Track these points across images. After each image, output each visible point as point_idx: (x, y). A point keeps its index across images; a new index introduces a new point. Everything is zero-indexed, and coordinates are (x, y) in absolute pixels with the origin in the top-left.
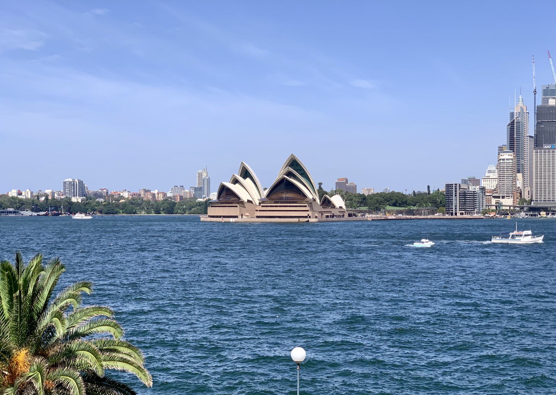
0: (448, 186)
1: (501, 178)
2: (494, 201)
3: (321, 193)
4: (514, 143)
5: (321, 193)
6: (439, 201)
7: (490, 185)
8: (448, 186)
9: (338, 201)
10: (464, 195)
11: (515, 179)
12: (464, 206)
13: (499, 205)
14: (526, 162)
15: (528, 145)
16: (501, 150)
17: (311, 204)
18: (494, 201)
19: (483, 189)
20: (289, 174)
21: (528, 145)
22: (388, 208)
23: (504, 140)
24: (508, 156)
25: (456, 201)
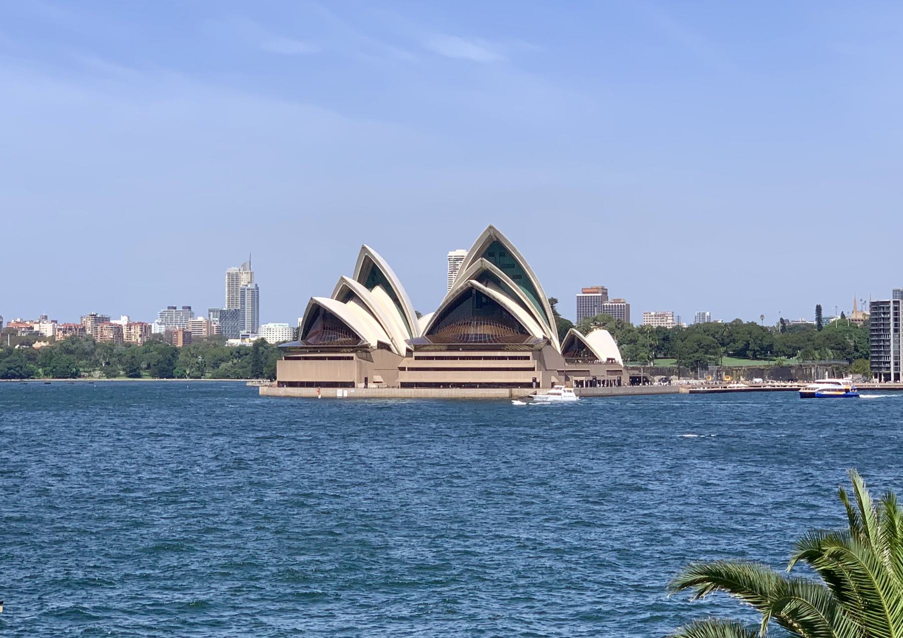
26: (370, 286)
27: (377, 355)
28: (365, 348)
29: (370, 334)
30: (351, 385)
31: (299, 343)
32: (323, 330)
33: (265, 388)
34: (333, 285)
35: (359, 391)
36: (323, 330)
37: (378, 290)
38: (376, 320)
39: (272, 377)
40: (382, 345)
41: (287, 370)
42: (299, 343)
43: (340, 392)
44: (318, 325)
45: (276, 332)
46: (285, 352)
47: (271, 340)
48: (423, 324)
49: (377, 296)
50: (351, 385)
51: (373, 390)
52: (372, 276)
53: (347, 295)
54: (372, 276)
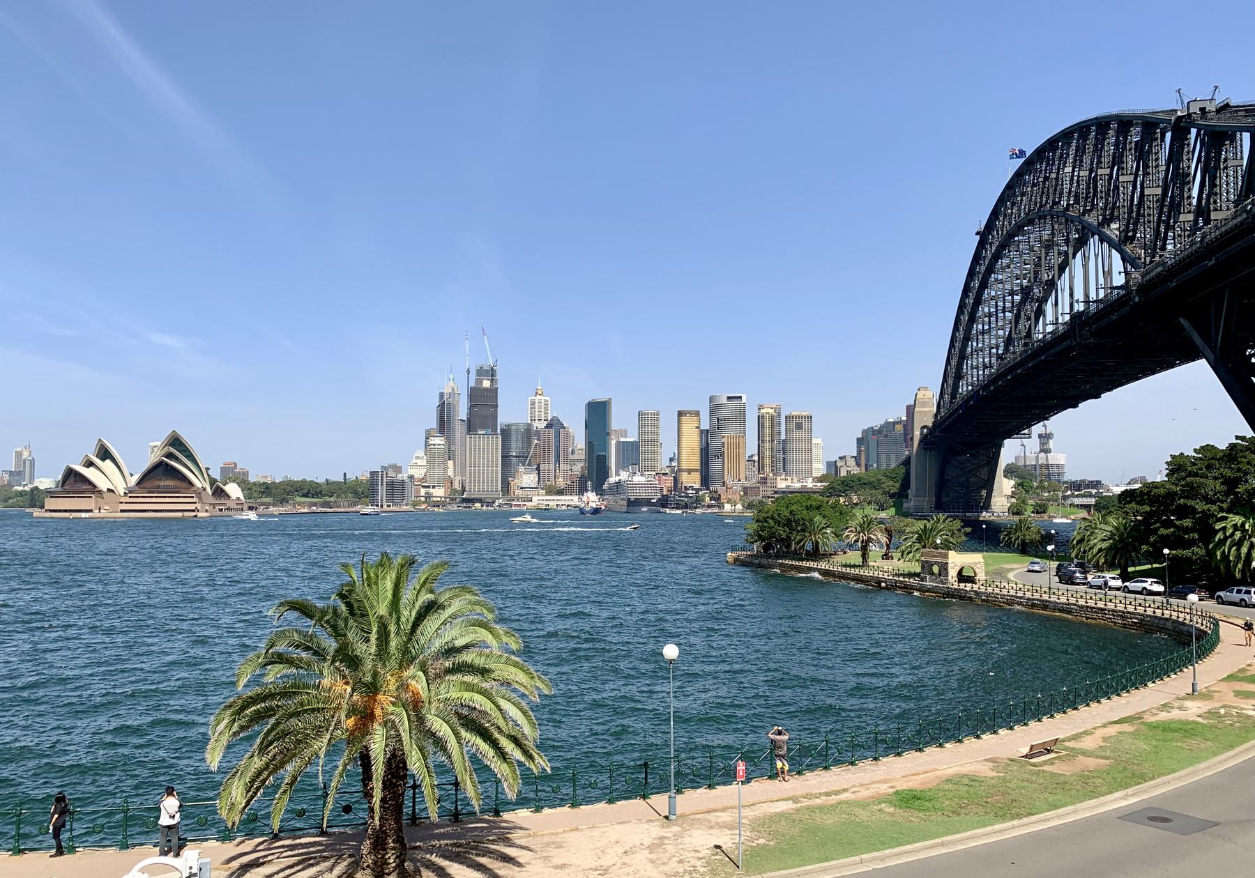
0: (373, 474)
1: (430, 464)
2: (423, 491)
3: (213, 482)
4: (444, 426)
5: (213, 482)
6: (363, 491)
7: (419, 473)
8: (373, 474)
9: (234, 490)
10: (391, 484)
11: (446, 467)
12: (391, 499)
13: (428, 496)
14: (457, 448)
15: (459, 430)
16: (429, 434)
17: (200, 493)
18: (423, 491)
19: (411, 477)
20: (170, 455)
21: (459, 430)
22: (299, 499)
23: (433, 423)
24: (438, 441)
25: (382, 491)
26: (103, 459)
27: (106, 495)
28: (100, 492)
29: (102, 484)
30: (91, 511)
31: (59, 489)
32: (74, 482)
33: (37, 513)
34: (81, 458)
35: (96, 514)
36: (74, 482)
37: (108, 461)
38: (104, 477)
39: (42, 507)
40: (109, 490)
41: (50, 503)
42: (59, 489)
43: (84, 515)
44: (72, 479)
45: (45, 482)
46: (50, 493)
47: (42, 487)
48: (133, 481)
49: (107, 465)
50: (91, 511)
51: (103, 513)
52: (105, 454)
53: (90, 464)
54: (105, 454)
